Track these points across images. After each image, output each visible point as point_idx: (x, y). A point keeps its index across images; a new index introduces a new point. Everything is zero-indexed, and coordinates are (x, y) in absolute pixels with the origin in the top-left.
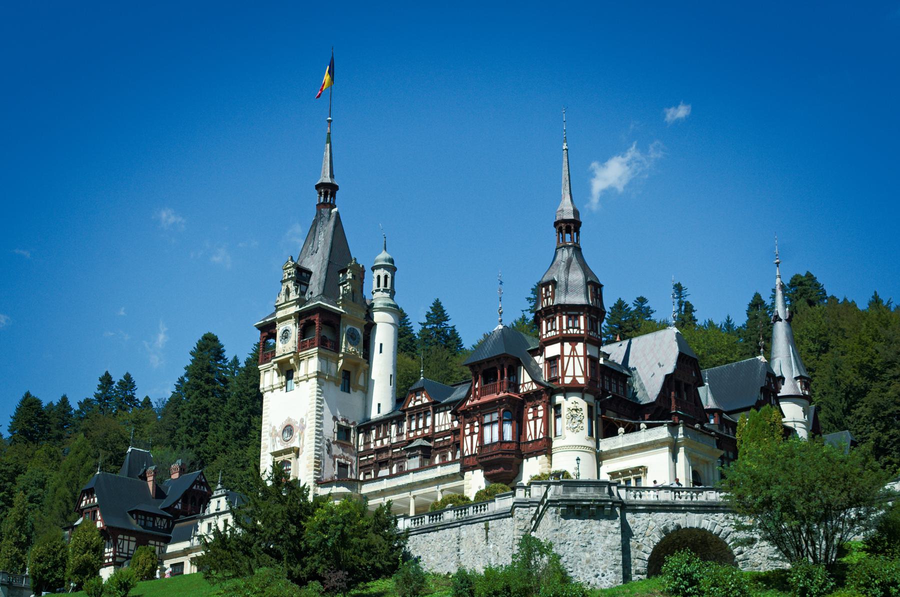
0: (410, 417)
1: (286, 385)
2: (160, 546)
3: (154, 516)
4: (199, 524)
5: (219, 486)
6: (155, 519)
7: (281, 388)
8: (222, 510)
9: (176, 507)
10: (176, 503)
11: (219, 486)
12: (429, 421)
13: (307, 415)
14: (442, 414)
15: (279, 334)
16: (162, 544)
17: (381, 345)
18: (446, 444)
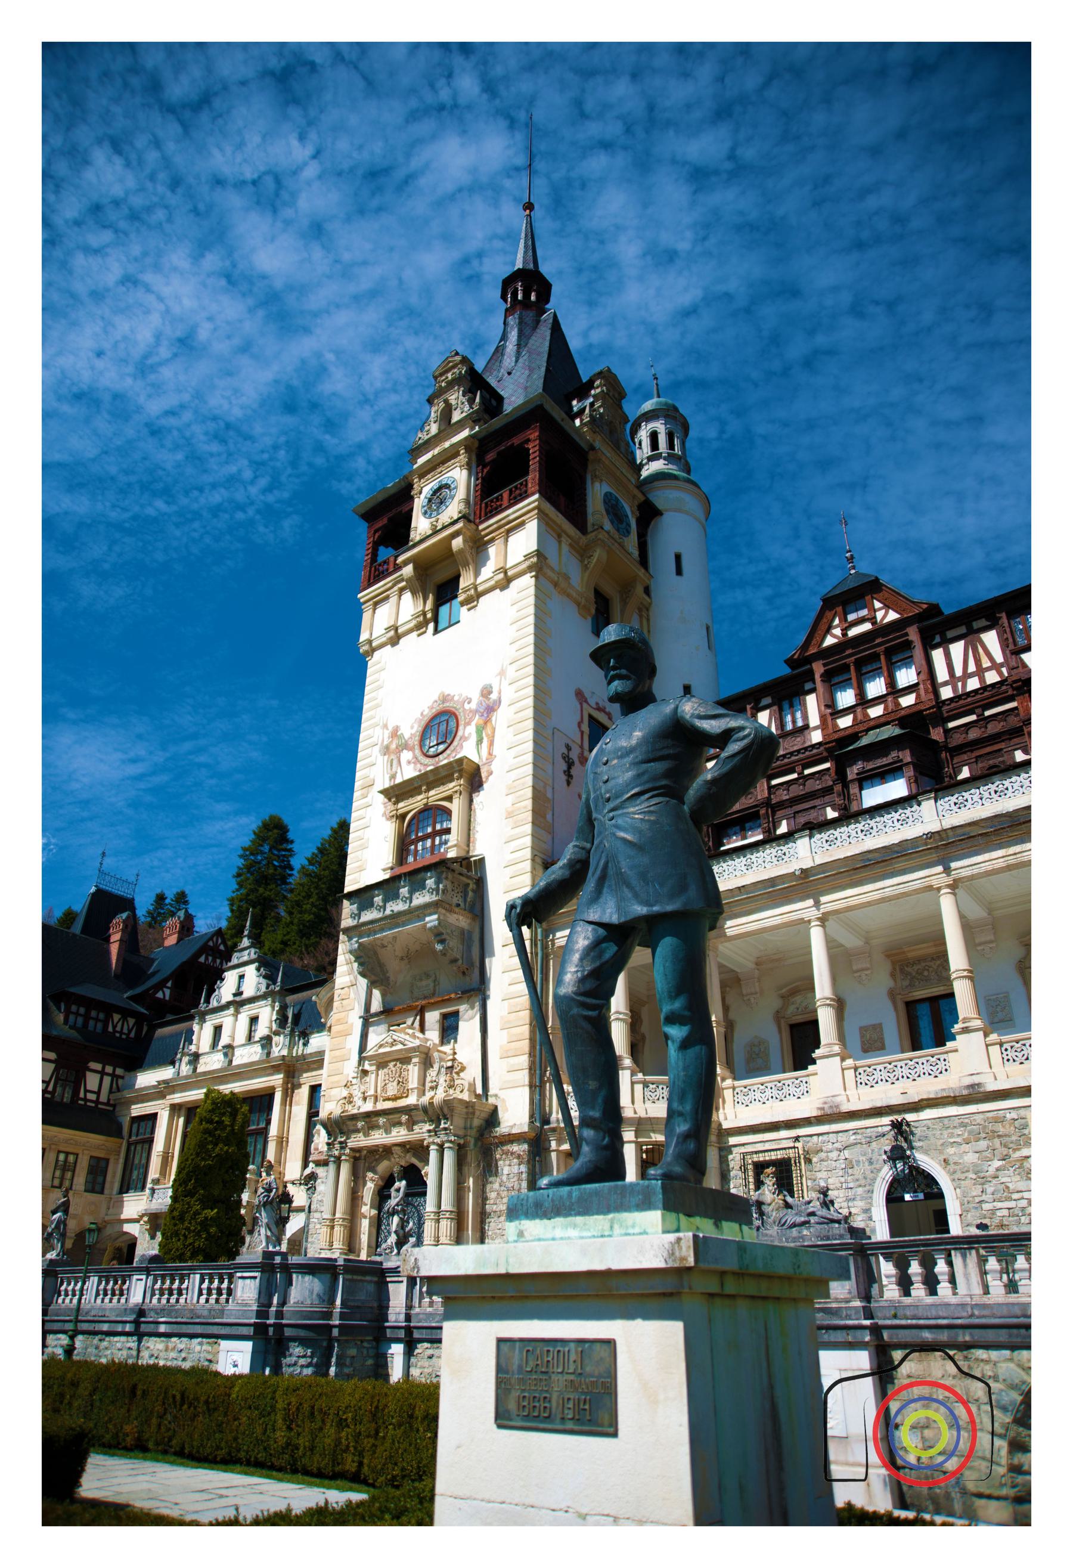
0: (827, 676)
1: (436, 619)
2: (113, 1075)
3: (109, 1009)
4: (196, 1028)
5: (246, 942)
6: (109, 1017)
7: (418, 627)
8: (246, 995)
9: (160, 995)
10: (161, 985)
11: (246, 942)
12: (906, 676)
13: (502, 673)
14: (957, 649)
15: (419, 503)
16: (119, 1071)
17: (678, 558)
18: (993, 728)
